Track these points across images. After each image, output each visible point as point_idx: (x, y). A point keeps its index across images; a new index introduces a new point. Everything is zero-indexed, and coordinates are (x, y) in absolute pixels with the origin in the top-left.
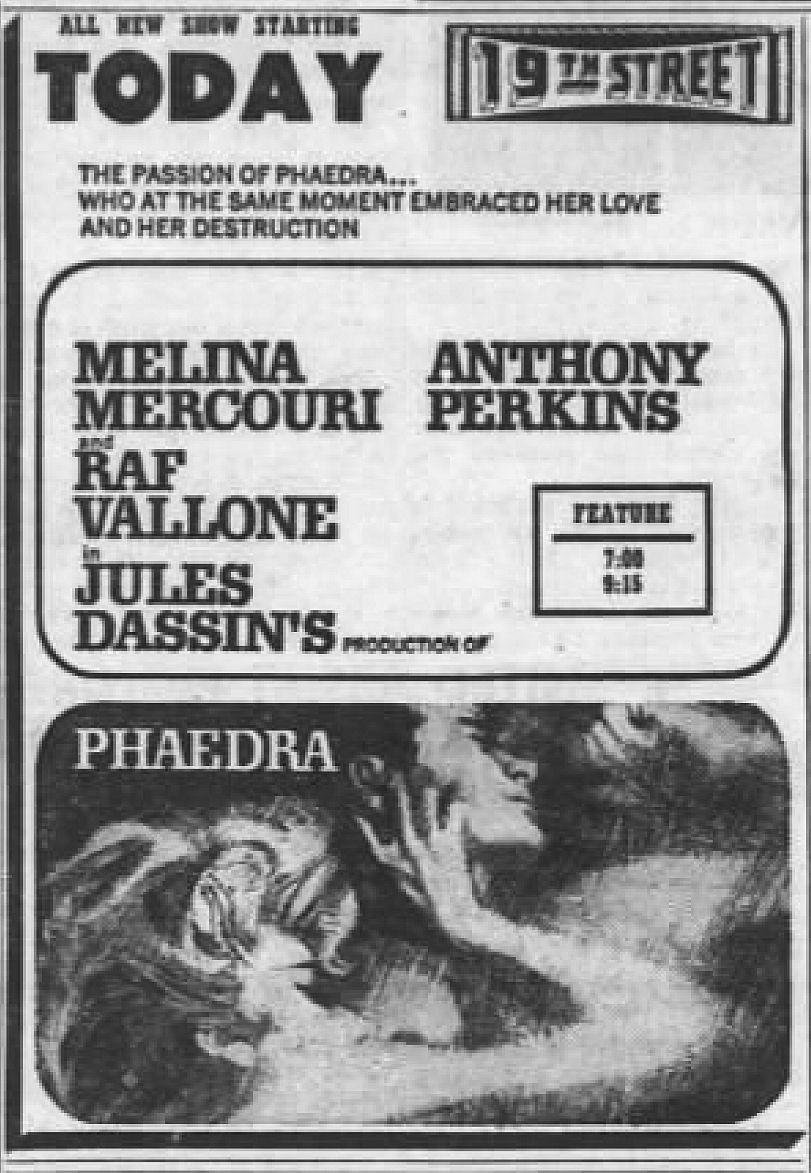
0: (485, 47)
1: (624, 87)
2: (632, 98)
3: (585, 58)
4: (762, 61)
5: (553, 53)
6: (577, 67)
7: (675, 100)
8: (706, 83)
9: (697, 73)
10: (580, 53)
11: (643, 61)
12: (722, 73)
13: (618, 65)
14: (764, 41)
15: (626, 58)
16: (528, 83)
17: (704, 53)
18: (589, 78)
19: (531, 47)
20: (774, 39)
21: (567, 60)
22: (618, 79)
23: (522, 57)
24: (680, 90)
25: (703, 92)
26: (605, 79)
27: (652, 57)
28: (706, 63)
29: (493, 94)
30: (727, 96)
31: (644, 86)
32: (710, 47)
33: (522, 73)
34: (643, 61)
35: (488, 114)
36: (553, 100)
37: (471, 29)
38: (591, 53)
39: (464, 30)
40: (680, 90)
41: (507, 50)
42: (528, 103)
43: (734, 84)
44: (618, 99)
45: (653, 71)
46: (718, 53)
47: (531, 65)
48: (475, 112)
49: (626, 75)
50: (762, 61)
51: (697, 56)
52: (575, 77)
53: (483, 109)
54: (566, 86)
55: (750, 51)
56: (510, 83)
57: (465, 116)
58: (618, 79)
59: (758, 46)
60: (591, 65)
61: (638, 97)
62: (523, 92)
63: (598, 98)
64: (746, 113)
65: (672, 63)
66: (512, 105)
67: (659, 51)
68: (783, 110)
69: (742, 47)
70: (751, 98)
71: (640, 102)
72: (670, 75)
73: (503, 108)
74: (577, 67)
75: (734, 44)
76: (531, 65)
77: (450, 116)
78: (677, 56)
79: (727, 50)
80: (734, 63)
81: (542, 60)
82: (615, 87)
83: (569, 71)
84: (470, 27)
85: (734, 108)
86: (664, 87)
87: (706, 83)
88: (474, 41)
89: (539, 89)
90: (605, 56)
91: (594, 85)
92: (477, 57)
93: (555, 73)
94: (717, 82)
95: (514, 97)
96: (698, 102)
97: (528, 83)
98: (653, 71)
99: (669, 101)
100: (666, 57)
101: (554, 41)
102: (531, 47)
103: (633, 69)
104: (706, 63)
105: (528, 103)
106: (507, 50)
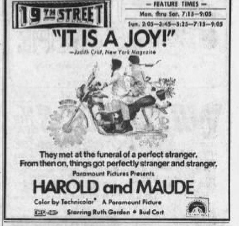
0: (23, 8)
1: (62, 18)
2: (64, 21)
3: (51, 10)
4: (102, 10)
5: (42, 9)
6: (49, 13)
7: (77, 21)
8: (86, 17)
9: (84, 14)
10: (49, 9)
11: (68, 11)
12: (91, 14)
13: (61, 12)
14: (103, 5)
15: (63, 10)
16: (35, 18)
17: (85, 9)
18: (52, 16)
19: (35, 7)
20: (106, 4)
21: (46, 11)
22: (61, 16)
23: (33, 10)
24: (79, 19)
25: (86, 20)
26: (57, 16)
27: (71, 10)
28: (86, 11)
29: (25, 21)
30: (92, 21)
31: (68, 18)
32: (87, 7)
33: (33, 15)
34: (68, 11)
35: (23, 27)
36: (42, 22)
37: (18, 3)
38: (53, 9)
39: (17, 3)
40: (79, 19)
41: (29, 9)
42: (34, 24)
43: (95, 17)
44: (61, 22)
45: (71, 13)
46: (90, 9)
47: (36, 12)
48: (20, 26)
49: (63, 15)
50: (102, 10)
51: (84, 9)
52: (48, 15)
53: (22, 25)
54: (46, 18)
55: (99, 8)
56: (30, 17)
57: (17, 27)
58: (61, 16)
59: (101, 6)
60: (53, 12)
61: (66, 21)
62: (33, 20)
63: (55, 22)
64: (98, 25)
65: (77, 12)
66: (30, 24)
67: (72, 8)
68: (108, 24)
69: (97, 7)
70: (99, 21)
71: (67, 23)
72: (76, 15)
73: (28, 25)
74: (49, 13)
75: (94, 6)
76: (36, 12)
77: (13, 27)
78: (78, 10)
79: (92, 8)
80: (95, 11)
81: (39, 11)
82: (60, 18)
83: (47, 14)
84: (18, 2)
85: (95, 24)
86: (74, 18)
87: (86, 17)
88: (19, 6)
89: (38, 19)
90: (57, 10)
91: (54, 18)
92: (20, 11)
93: (43, 15)
94: (90, 17)
95: (31, 21)
96: (84, 22)
97: (35, 18)
98: (71, 13)
99: (76, 22)
100: (74, 10)
101: (43, 5)
102: (35, 7)
103: (65, 14)
104: (86, 11)
105: (34, 24)
106: (29, 9)
